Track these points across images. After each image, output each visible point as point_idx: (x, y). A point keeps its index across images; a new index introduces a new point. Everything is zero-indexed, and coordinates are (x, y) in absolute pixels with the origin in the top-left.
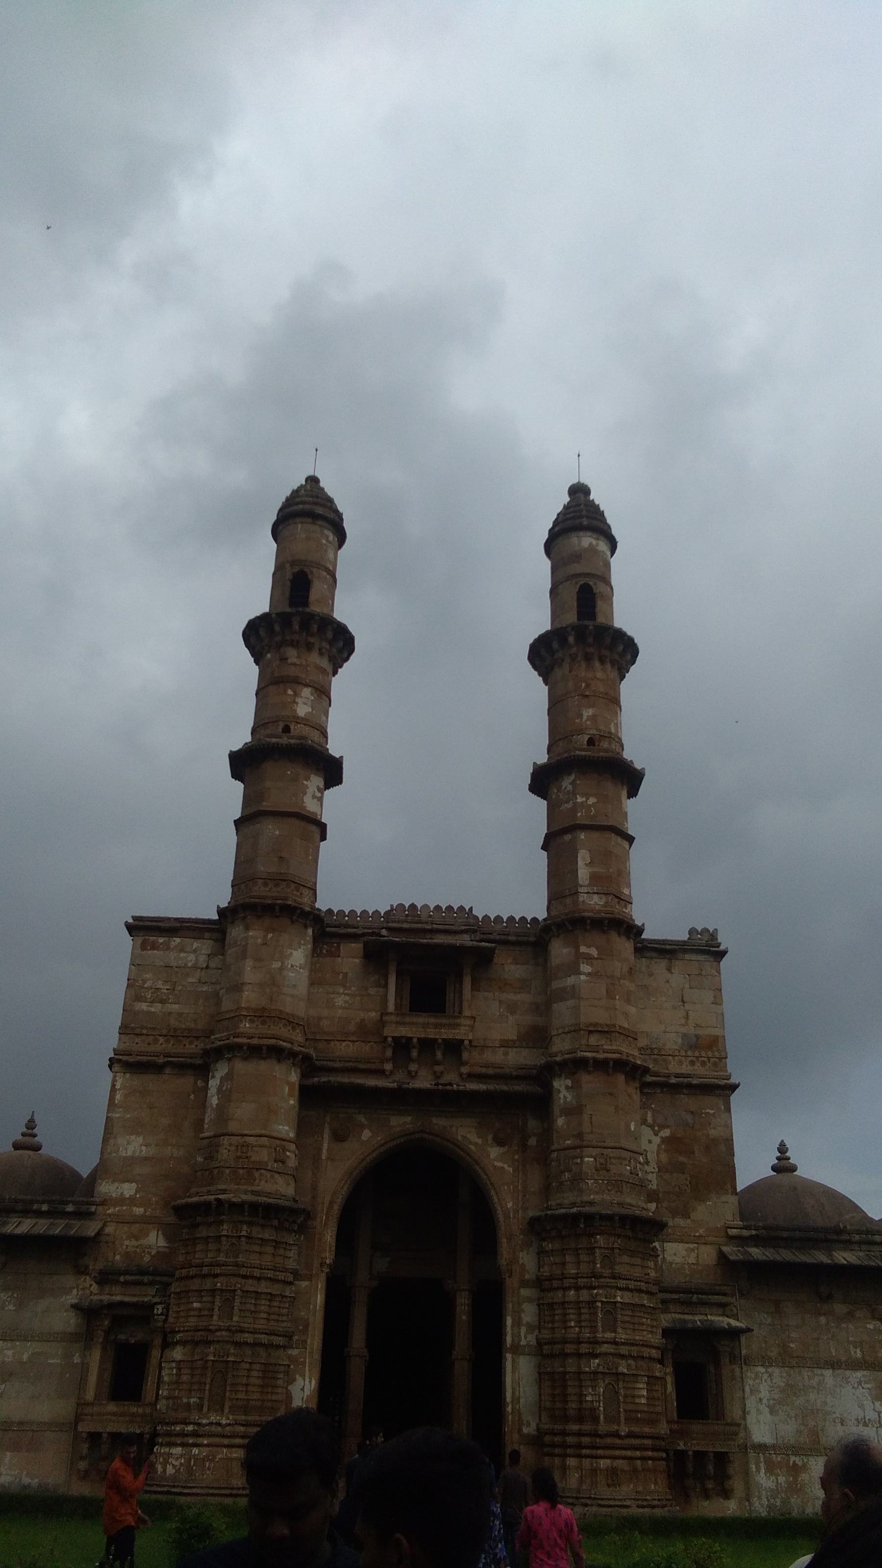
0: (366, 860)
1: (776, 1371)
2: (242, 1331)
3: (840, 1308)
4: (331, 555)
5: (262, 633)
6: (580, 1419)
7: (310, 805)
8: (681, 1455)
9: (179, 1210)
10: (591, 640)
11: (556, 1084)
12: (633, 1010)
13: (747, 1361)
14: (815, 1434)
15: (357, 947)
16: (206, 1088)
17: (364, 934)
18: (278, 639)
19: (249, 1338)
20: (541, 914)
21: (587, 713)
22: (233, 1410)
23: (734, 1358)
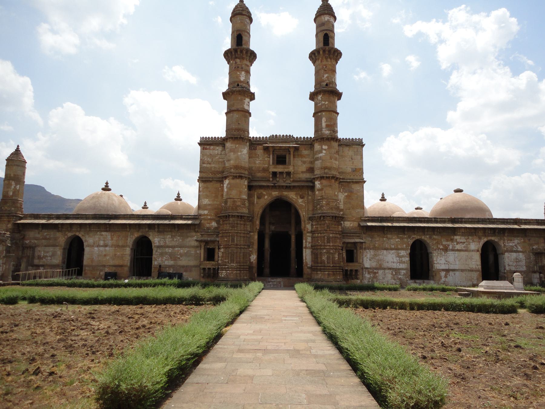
0: (262, 125)
1: (372, 251)
2: (237, 245)
3: (389, 236)
5: (229, 55)
6: (321, 263)
7: (246, 107)
8: (347, 270)
10: (327, 52)
11: (316, 183)
12: (337, 162)
13: (365, 249)
14: (381, 265)
16: (223, 186)
18: (234, 56)
20: (313, 136)
21: (326, 76)
22: (236, 263)
23: (361, 248)
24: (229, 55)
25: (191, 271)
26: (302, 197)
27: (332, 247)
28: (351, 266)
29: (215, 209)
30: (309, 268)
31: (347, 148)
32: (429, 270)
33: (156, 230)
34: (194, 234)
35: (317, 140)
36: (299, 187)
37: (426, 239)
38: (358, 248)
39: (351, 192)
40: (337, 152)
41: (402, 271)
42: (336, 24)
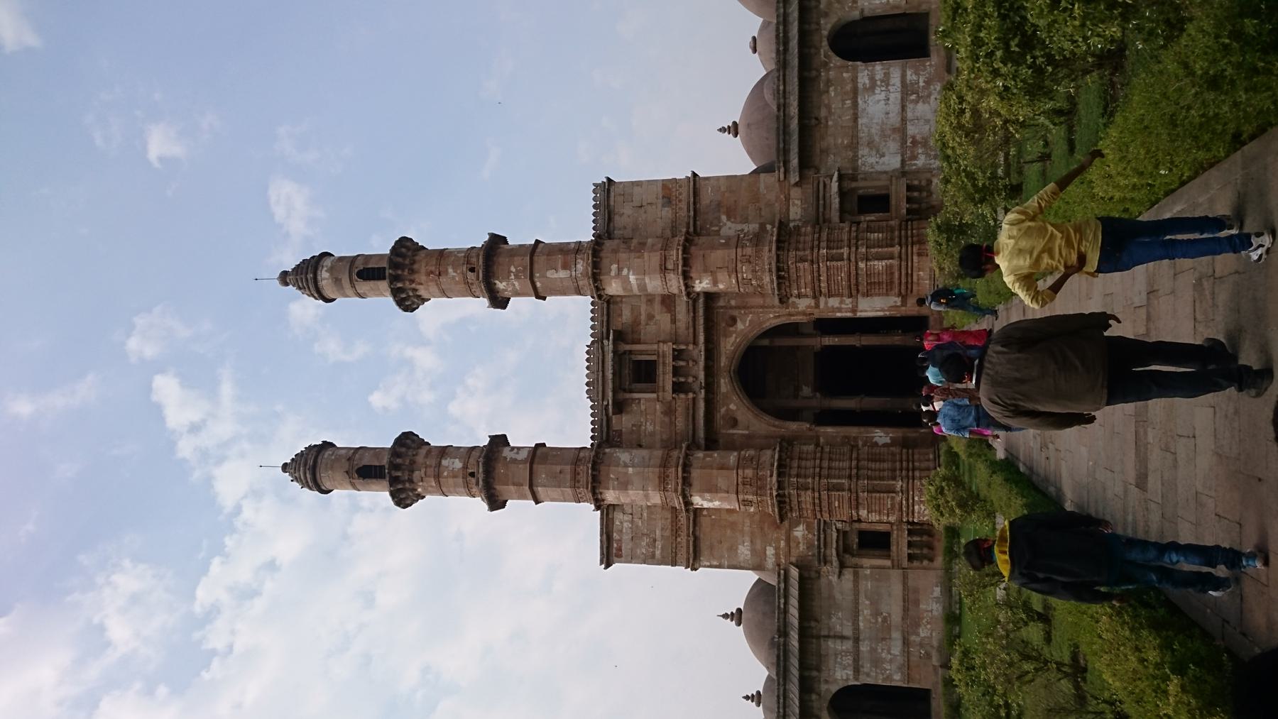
3: (823, 113)
4: (343, 452)
5: (403, 496)
6: (892, 274)
9: (782, 520)
13: (855, 169)
14: (894, 130)
15: (614, 419)
17: (607, 415)
19: (854, 471)
23: (854, 178)
24: (403, 496)
25: (916, 591)
26: (733, 320)
27: (853, 249)
28: (900, 204)
29: (762, 529)
30: (904, 303)
31: (617, 218)
32: (904, 15)
33: (815, 673)
34: (823, 581)
35: (597, 289)
36: (708, 330)
37: (829, 26)
38: (854, 185)
39: (719, 205)
40: (626, 240)
41: (909, 77)
42: (337, 255)
